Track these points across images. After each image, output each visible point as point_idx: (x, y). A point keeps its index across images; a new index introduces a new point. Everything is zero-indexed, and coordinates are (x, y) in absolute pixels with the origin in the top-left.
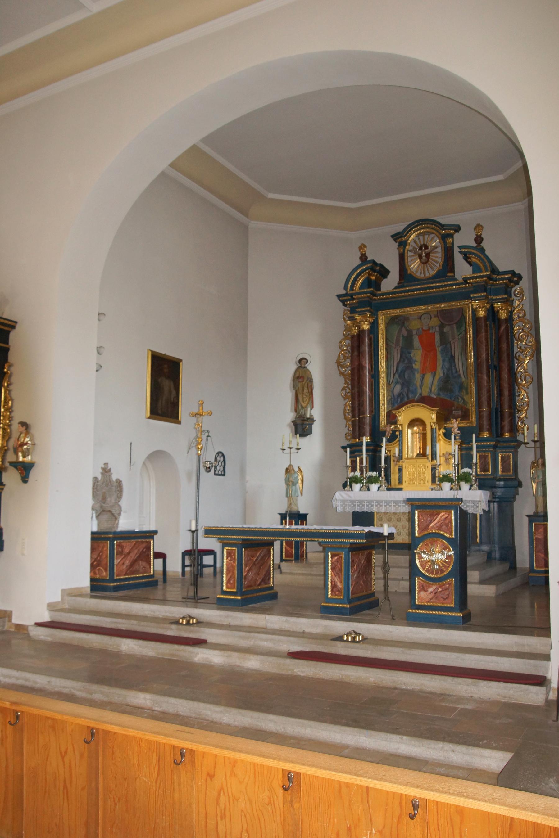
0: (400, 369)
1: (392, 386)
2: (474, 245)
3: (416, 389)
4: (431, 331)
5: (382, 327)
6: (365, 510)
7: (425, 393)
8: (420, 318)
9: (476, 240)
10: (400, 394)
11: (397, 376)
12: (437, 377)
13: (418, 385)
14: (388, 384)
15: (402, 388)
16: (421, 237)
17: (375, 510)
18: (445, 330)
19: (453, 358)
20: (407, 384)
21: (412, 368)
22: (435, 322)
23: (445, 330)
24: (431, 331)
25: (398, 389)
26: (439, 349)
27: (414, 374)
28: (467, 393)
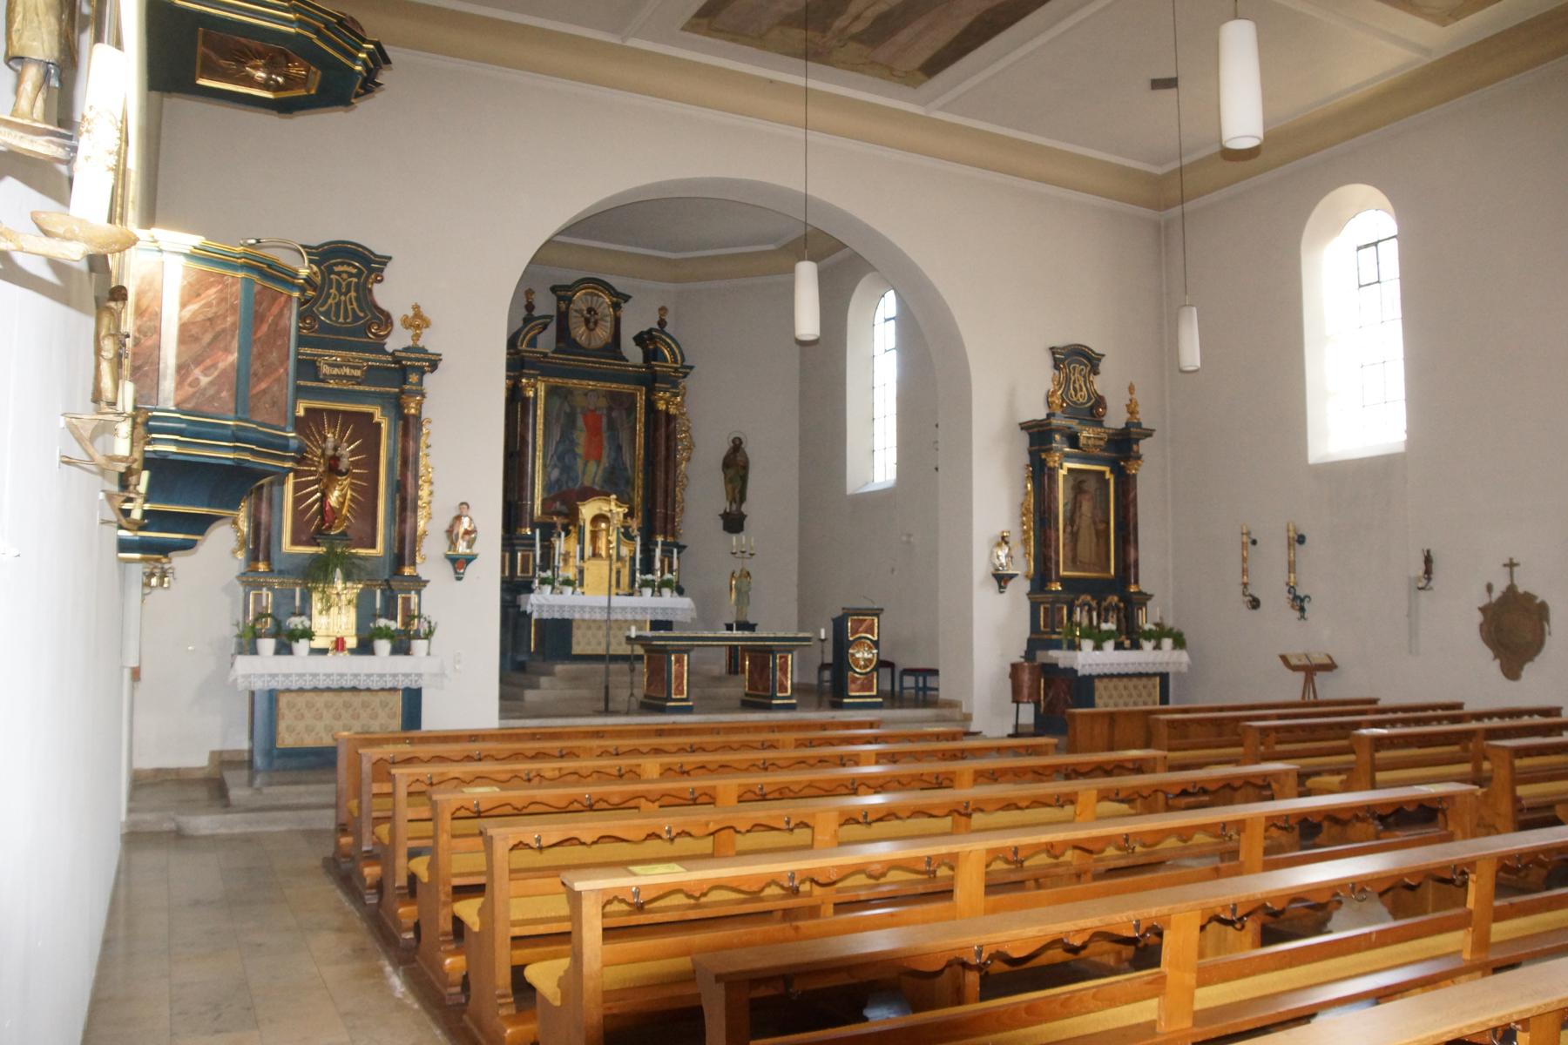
0: (561, 449)
1: (549, 469)
2: (657, 327)
3: (577, 477)
4: (598, 412)
5: (542, 393)
6: (567, 616)
7: (587, 483)
8: (586, 395)
9: (659, 324)
10: (558, 481)
11: (555, 458)
12: (602, 467)
13: (580, 473)
14: (545, 466)
15: (561, 474)
16: (589, 298)
17: (577, 616)
18: (614, 414)
19: (619, 448)
20: (567, 469)
21: (574, 451)
22: (603, 403)
23: (614, 414)
24: (598, 412)
25: (555, 474)
26: (605, 435)
27: (575, 459)
28: (634, 490)
